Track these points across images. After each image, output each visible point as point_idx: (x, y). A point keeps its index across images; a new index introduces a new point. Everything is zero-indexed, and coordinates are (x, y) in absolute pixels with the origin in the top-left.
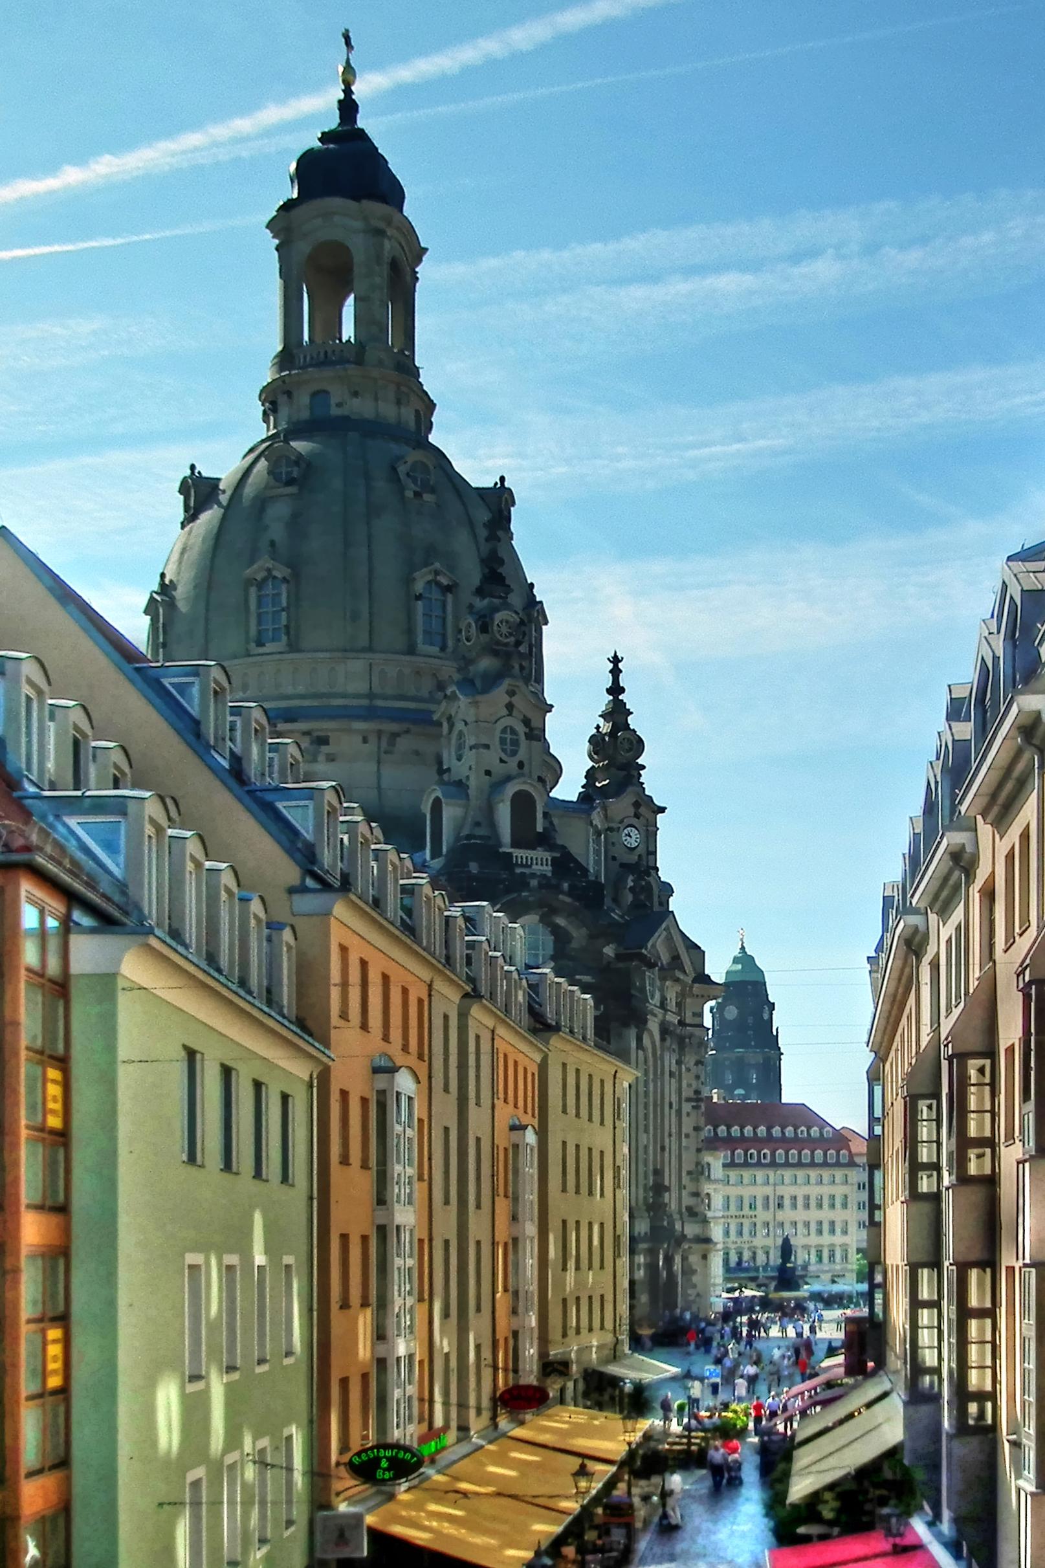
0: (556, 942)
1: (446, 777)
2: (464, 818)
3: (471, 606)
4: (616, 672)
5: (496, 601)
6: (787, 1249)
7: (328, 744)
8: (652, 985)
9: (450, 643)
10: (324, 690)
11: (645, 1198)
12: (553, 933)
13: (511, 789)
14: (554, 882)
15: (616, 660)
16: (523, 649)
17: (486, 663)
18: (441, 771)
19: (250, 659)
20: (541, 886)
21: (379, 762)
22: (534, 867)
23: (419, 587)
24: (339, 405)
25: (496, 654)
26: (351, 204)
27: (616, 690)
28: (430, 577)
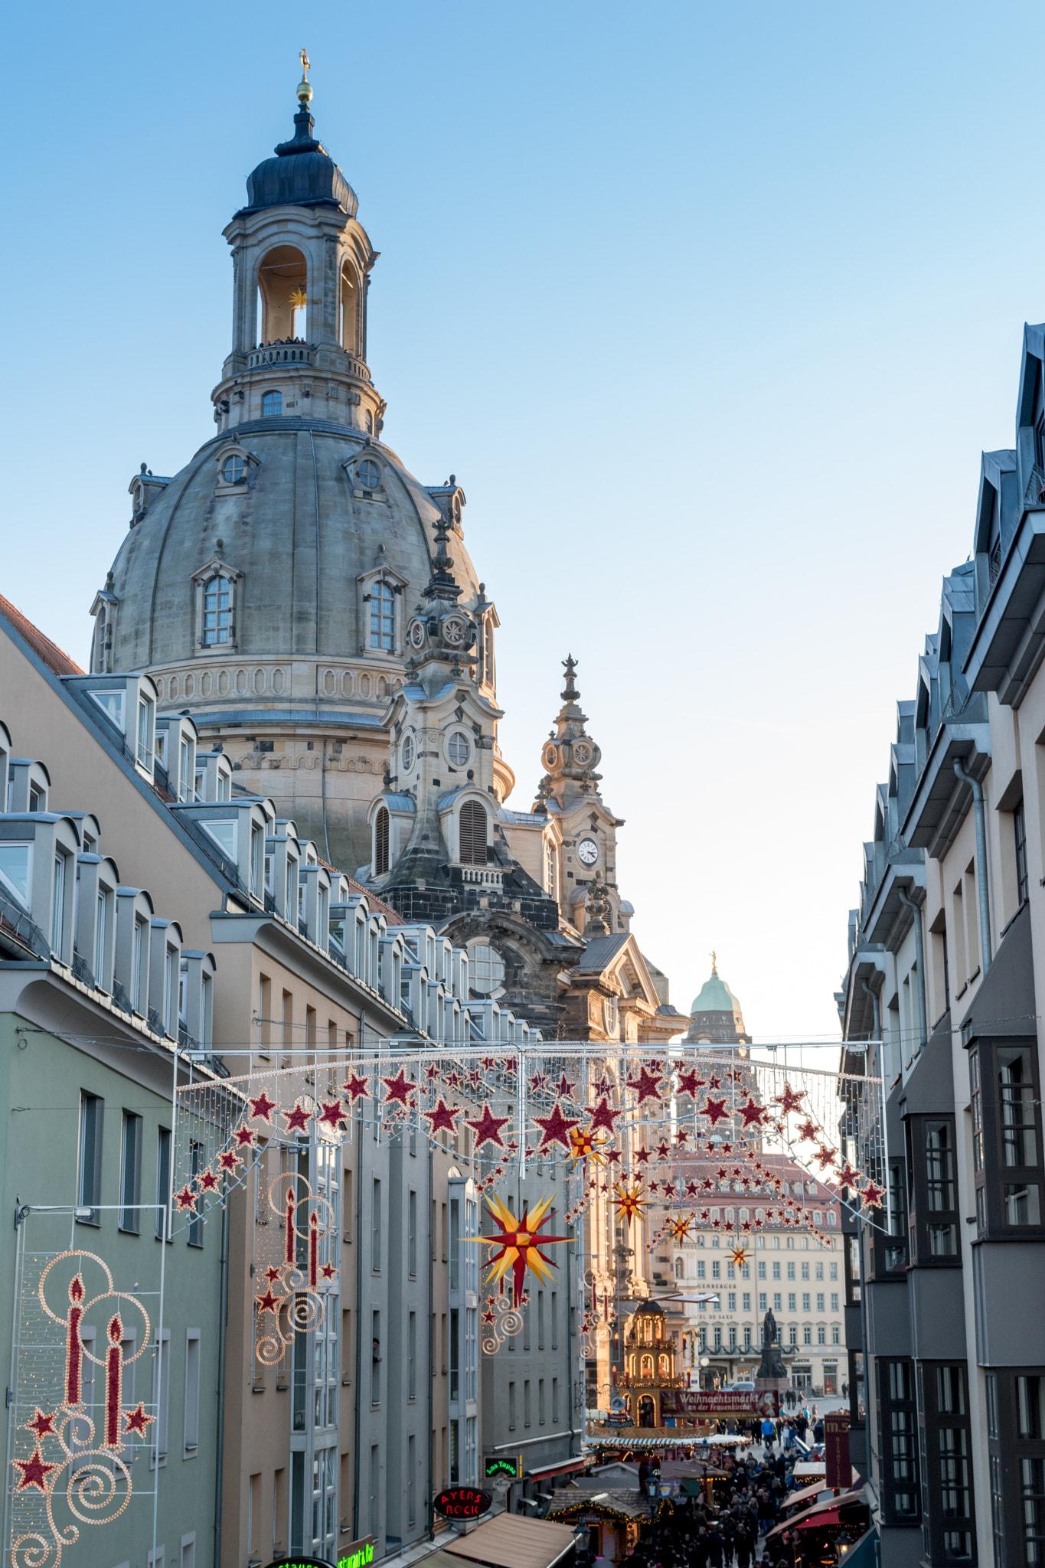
0: (508, 966)
1: (392, 786)
2: (413, 830)
3: (419, 609)
4: (570, 676)
5: (446, 603)
6: (770, 1329)
7: (271, 749)
8: (613, 1017)
9: (398, 646)
10: (268, 694)
11: (609, 1262)
12: (504, 956)
13: (460, 801)
14: (506, 900)
15: (570, 664)
16: (473, 652)
17: (432, 668)
18: (388, 780)
19: (194, 662)
20: (491, 905)
21: (324, 771)
22: (484, 884)
23: (369, 587)
24: (288, 405)
25: (445, 658)
26: (305, 213)
27: (570, 695)
28: (378, 578)
